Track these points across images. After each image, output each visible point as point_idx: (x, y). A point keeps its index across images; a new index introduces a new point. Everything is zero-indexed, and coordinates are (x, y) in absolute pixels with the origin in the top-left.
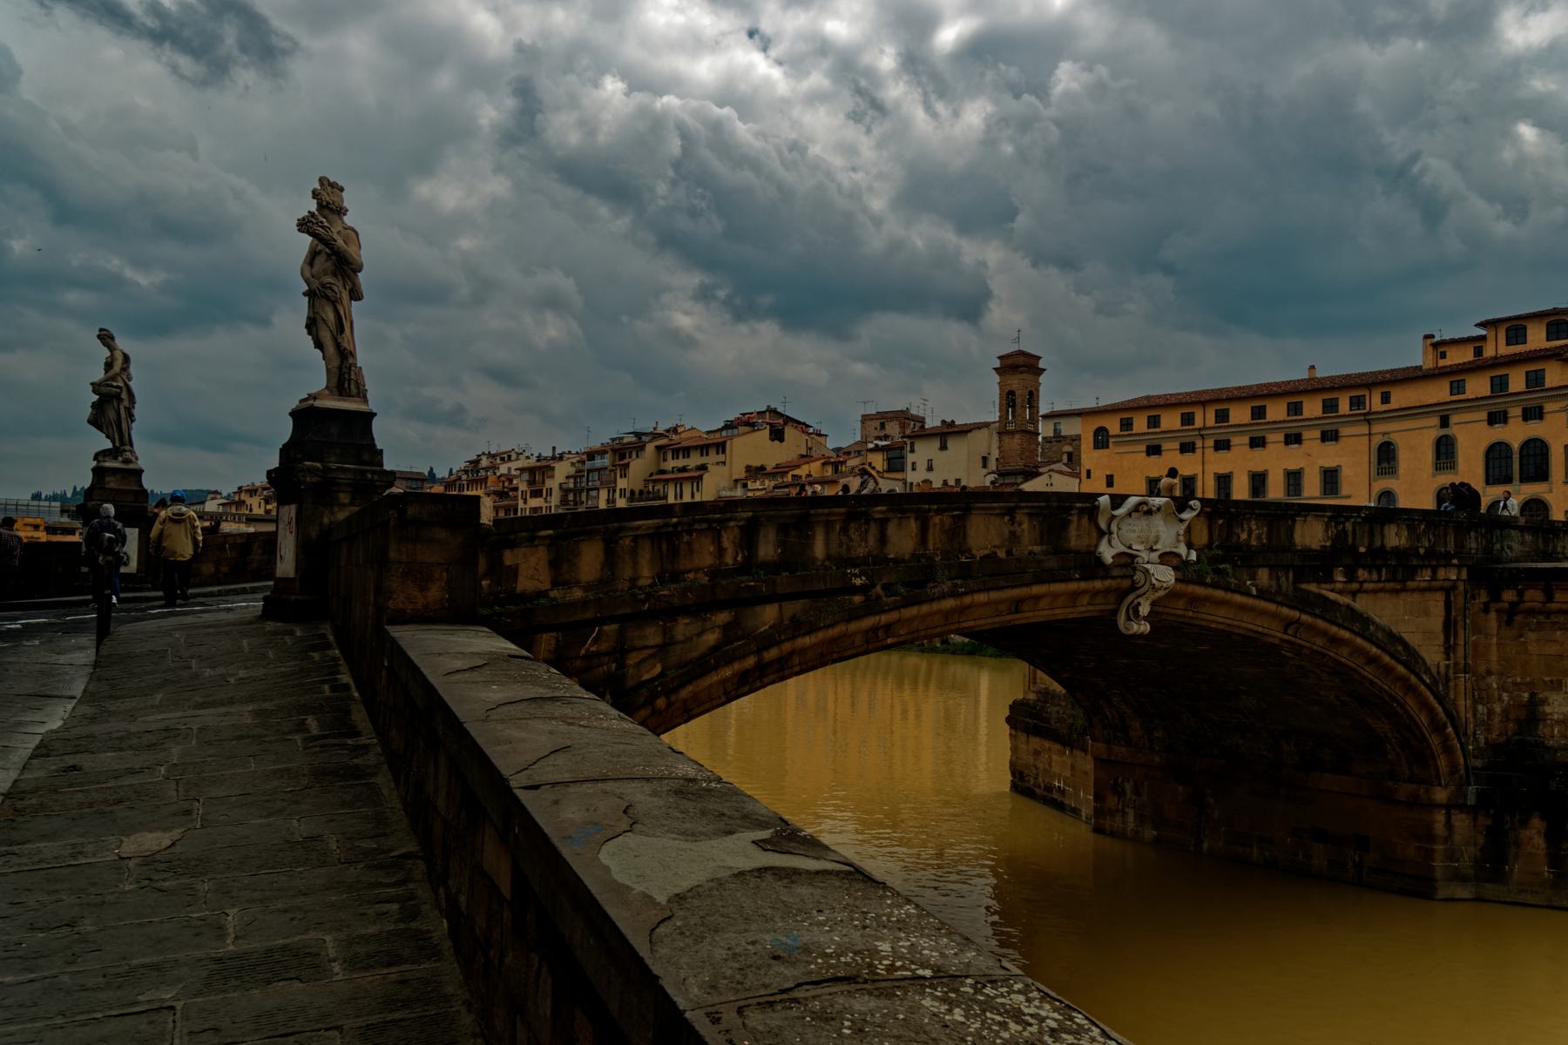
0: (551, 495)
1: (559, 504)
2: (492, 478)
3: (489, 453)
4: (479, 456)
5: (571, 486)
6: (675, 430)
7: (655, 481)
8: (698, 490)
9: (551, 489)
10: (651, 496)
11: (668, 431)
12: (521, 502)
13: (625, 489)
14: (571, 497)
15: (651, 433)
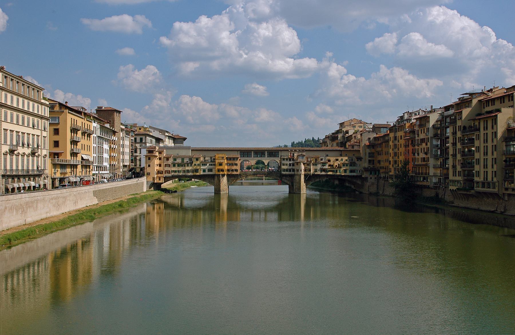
0: (428, 132)
1: (433, 136)
2: (407, 125)
3: (409, 112)
4: (404, 114)
5: (439, 126)
6: (491, 90)
7: (474, 120)
8: (495, 124)
9: (428, 128)
10: (473, 129)
11: (488, 91)
12: (416, 136)
13: (460, 126)
14: (439, 132)
15: (481, 93)
